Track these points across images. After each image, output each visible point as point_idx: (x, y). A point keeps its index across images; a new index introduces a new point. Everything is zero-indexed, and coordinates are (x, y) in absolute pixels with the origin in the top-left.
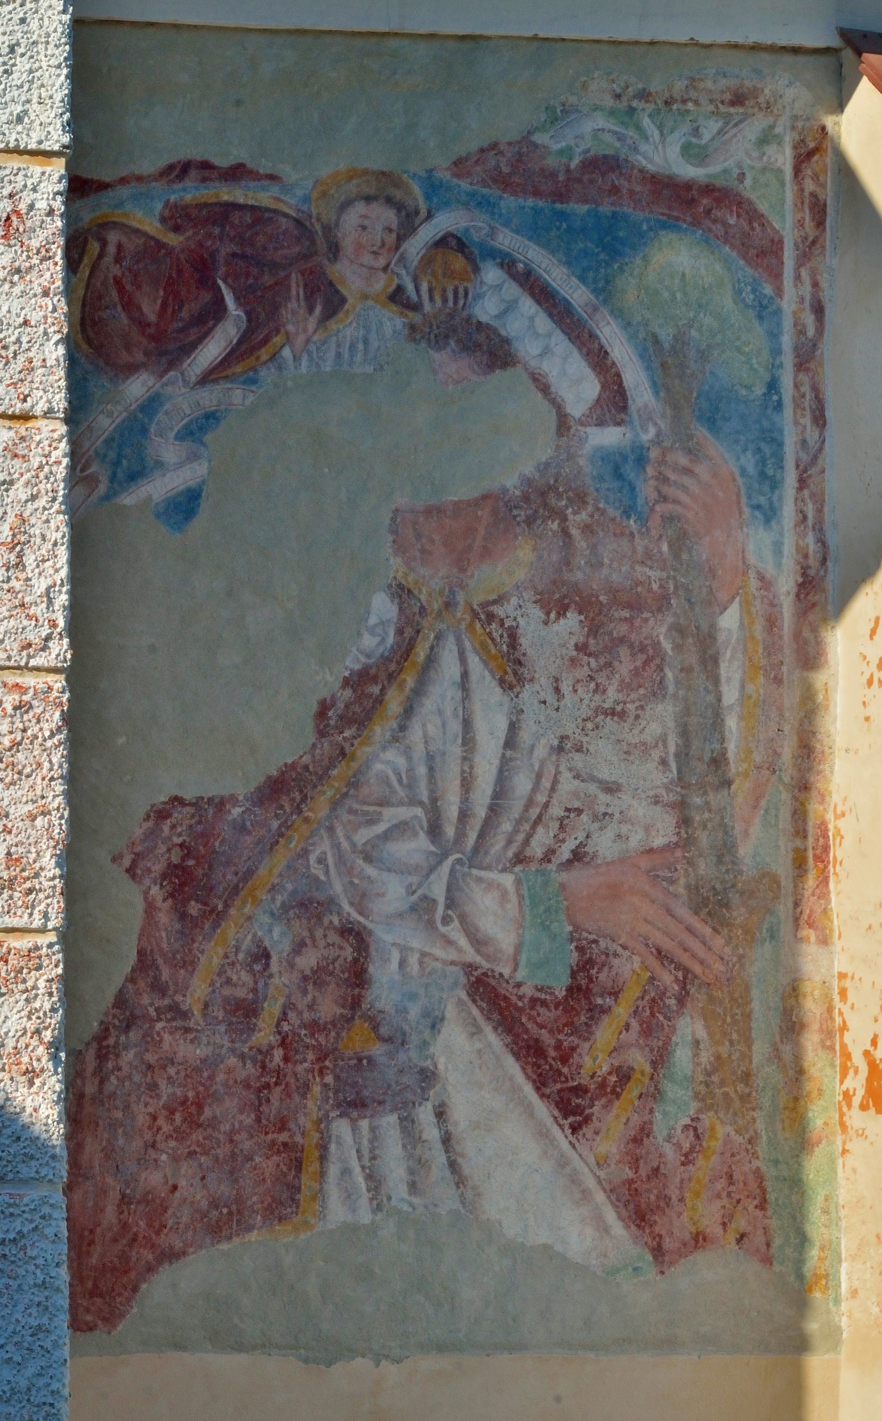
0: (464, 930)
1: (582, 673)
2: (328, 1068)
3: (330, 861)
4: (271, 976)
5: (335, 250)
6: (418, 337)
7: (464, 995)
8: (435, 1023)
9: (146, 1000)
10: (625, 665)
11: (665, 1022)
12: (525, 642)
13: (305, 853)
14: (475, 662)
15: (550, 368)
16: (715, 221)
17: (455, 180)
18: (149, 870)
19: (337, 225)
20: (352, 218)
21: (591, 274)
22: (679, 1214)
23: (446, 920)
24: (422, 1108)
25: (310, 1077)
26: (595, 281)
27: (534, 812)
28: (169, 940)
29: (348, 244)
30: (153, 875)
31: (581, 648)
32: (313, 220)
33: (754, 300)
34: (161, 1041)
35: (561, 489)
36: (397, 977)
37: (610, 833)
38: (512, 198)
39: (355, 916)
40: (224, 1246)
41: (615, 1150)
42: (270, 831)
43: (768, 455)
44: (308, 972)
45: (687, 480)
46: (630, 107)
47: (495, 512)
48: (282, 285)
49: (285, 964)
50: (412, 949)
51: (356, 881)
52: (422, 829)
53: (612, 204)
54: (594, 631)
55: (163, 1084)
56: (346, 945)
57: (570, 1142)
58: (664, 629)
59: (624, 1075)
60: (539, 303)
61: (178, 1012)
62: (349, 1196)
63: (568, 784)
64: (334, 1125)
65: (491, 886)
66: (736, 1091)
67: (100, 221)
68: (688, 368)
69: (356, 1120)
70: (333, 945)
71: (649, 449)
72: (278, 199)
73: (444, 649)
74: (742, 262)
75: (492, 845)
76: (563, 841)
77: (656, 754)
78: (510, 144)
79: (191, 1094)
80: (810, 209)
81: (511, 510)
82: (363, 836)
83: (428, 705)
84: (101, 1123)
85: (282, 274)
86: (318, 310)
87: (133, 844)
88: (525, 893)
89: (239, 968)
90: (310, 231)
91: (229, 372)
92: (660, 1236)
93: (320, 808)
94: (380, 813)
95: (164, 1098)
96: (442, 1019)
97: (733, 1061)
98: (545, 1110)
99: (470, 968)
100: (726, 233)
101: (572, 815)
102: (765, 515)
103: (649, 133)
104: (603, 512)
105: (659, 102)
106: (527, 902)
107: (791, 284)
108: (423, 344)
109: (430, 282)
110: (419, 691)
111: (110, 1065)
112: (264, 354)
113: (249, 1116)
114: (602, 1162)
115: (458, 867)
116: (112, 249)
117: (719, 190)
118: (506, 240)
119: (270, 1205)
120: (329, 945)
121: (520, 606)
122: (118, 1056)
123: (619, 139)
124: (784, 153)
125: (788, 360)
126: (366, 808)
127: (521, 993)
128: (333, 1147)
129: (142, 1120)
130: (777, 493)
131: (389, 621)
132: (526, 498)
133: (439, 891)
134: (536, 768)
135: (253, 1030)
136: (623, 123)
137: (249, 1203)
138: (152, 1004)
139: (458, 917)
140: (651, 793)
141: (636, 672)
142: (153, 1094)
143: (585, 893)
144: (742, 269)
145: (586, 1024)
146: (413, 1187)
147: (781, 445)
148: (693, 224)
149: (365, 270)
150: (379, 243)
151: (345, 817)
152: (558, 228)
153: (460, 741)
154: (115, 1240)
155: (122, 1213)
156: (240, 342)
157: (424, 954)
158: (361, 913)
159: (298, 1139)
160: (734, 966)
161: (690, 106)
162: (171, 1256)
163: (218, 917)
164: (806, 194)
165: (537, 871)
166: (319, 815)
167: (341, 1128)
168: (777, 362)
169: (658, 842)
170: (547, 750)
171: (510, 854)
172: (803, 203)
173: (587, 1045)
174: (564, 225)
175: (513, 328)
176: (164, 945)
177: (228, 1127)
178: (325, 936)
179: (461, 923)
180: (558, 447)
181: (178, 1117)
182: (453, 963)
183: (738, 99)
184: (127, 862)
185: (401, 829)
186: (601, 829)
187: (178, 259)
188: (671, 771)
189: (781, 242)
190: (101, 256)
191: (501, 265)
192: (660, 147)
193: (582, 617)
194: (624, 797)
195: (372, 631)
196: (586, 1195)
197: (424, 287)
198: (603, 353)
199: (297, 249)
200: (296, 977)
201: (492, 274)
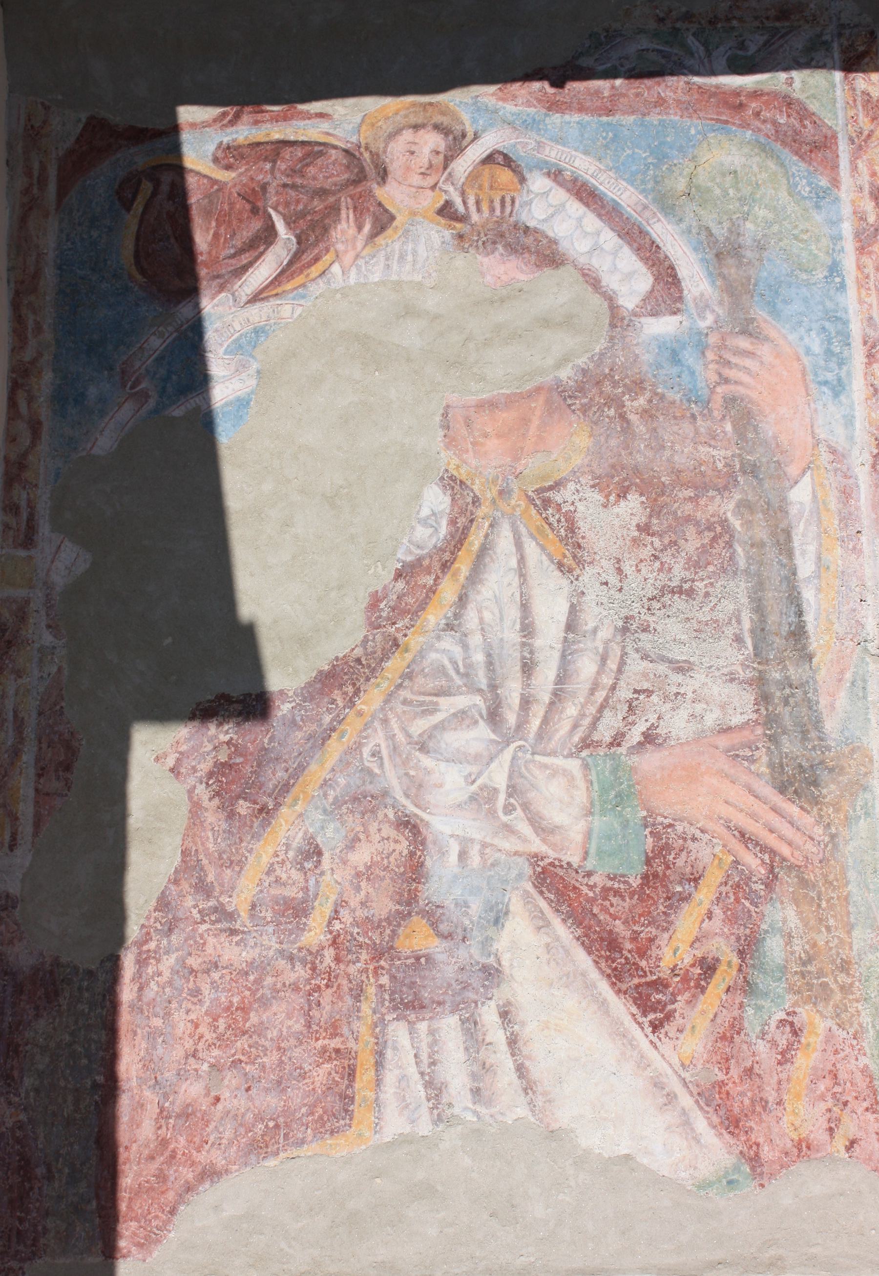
0: (528, 819)
1: (646, 553)
2: (383, 968)
3: (385, 753)
4: (322, 873)
5: (383, 175)
6: (466, 246)
7: (529, 887)
9: (189, 902)
10: (692, 543)
11: (752, 908)
12: (583, 526)
13: (359, 746)
14: (531, 548)
15: (601, 265)
16: (764, 121)
17: (500, 103)
18: (194, 770)
19: (385, 152)
21: (640, 177)
22: (779, 1119)
23: (509, 809)
24: (485, 1008)
25: (364, 978)
26: (643, 182)
27: (600, 696)
28: (216, 840)
29: (395, 167)
30: (198, 774)
31: (645, 528)
32: (362, 150)
33: (810, 192)
34: (204, 944)
35: (617, 377)
36: (456, 870)
37: (683, 714)
38: (558, 115)
39: (411, 808)
40: (272, 1162)
41: (701, 1049)
42: (321, 725)
43: (833, 334)
44: (361, 868)
45: (748, 362)
46: (674, 28)
47: (548, 402)
49: (337, 860)
50: (472, 840)
51: (412, 773)
52: (482, 717)
53: (659, 114)
54: (655, 509)
55: (206, 989)
56: (401, 838)
57: (651, 1042)
58: (731, 506)
59: (709, 967)
60: (587, 205)
61: (224, 914)
63: (636, 665)
64: (391, 1028)
65: (555, 772)
66: (836, 981)
67: (153, 164)
68: (744, 257)
69: (414, 1023)
70: (388, 839)
71: (707, 334)
72: (328, 134)
73: (498, 536)
74: (795, 158)
75: (557, 730)
76: (634, 723)
77: (730, 631)
78: (554, 68)
79: (236, 1000)
80: (863, 106)
81: (565, 399)
84: (139, 1031)
85: (331, 199)
86: (367, 228)
87: (178, 743)
88: (594, 777)
89: (289, 866)
90: (359, 159)
91: (279, 290)
92: (758, 1145)
94: (436, 704)
95: (208, 1004)
96: (507, 913)
97: (831, 949)
98: (622, 1007)
99: (535, 858)
100: (777, 131)
101: (642, 697)
102: (833, 389)
103: (694, 49)
104: (662, 397)
105: (703, 22)
106: (596, 786)
107: (848, 175)
108: (472, 251)
109: (477, 195)
111: (150, 970)
112: (314, 271)
113: (297, 1022)
114: (687, 1063)
115: (520, 754)
116: (165, 188)
117: (768, 94)
118: (553, 153)
119: (321, 1118)
120: (383, 839)
121: (578, 491)
122: (158, 961)
123: (664, 57)
124: (833, 57)
125: (849, 245)
126: (422, 698)
127: (591, 883)
128: (389, 1054)
129: (182, 1027)
130: (845, 368)
131: (443, 511)
132: (581, 388)
133: (500, 780)
134: (601, 650)
135: (304, 930)
136: (666, 43)
137: (298, 1115)
138: (195, 906)
139: (521, 805)
140: (725, 671)
141: (704, 550)
142: (195, 1000)
143: (658, 776)
144: (796, 165)
145: (664, 913)
146: (476, 1092)
147: (846, 323)
148: (741, 126)
149: (414, 190)
150: (426, 165)
151: (400, 708)
152: (605, 138)
153: (518, 627)
154: (152, 1158)
155: (160, 1128)
156: (291, 263)
157: (484, 845)
158: (416, 806)
159: (351, 1044)
160: (826, 846)
161: (735, 23)
163: (265, 813)
164: (858, 93)
165: (606, 755)
166: (373, 708)
168: (838, 248)
169: (737, 720)
170: (611, 630)
171: (576, 739)
172: (855, 101)
173: (666, 935)
174: (610, 134)
176: (211, 846)
177: (275, 1033)
178: (379, 830)
179: (524, 810)
180: (612, 338)
181: (222, 1024)
182: (516, 853)
183: (784, 14)
184: (171, 762)
185: (461, 717)
186: (673, 709)
187: (231, 193)
188: (746, 648)
189: (834, 137)
190: (154, 194)
191: (548, 174)
192: (706, 60)
193: (644, 499)
194: (697, 676)
195: (424, 522)
196: (671, 1098)
197: (471, 201)
198: (655, 247)
199: (346, 176)
200: (349, 873)
201: (538, 183)
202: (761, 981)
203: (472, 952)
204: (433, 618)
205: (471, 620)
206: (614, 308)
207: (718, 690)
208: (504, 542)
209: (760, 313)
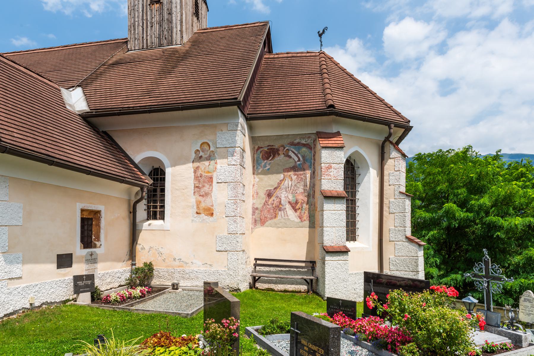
5: (279, 151)
8: (286, 205)
15: (294, 158)
20: (280, 148)
29: (280, 150)
59: (299, 208)
62: (280, 217)
63: (296, 188)
83: (285, 183)
93: (278, 190)
110: (285, 181)
118: (291, 149)
162: (267, 221)
163: (271, 198)
167: (279, 212)
175: (292, 155)
201: (290, 151)
202: (303, 209)
203: (284, 207)
204: (282, 184)
205: (285, 184)
206: (295, 161)
207: (301, 190)
208: (287, 179)
209: (306, 162)
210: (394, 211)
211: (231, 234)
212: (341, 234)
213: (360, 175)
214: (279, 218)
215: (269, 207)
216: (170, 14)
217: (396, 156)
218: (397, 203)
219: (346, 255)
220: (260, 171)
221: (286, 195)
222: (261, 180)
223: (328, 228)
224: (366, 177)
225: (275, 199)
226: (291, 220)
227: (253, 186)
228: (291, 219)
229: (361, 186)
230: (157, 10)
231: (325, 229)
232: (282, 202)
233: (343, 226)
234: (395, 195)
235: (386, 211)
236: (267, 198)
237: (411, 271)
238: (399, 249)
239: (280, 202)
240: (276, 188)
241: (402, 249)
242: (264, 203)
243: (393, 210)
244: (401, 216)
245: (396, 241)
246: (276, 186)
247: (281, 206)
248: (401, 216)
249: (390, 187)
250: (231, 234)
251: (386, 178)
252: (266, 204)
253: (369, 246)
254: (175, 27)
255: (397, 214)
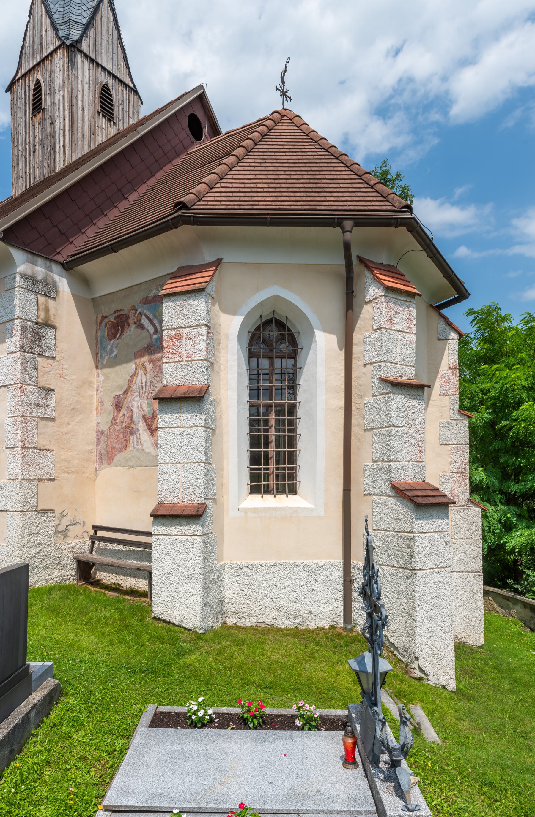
48: (124, 324)
82: (133, 397)
162: (116, 455)
163: (120, 410)
203: (137, 427)
204: (134, 383)
205: (137, 383)
208: (140, 372)
210: (373, 425)
211: (11, 479)
212: (195, 478)
213: (302, 349)
214: (131, 449)
215: (117, 428)
216: (52, 123)
217: (376, 296)
218: (376, 405)
219: (195, 524)
220: (105, 362)
221: (139, 404)
222: (107, 377)
223: (166, 465)
224: (311, 351)
225: (126, 412)
226: (146, 453)
227: (97, 390)
228: (146, 450)
229: (303, 373)
230: (39, 124)
231: (161, 468)
232: (135, 418)
233: (199, 461)
234: (373, 386)
235: (359, 425)
236: (116, 411)
237: (402, 568)
238: (379, 513)
239: (132, 417)
240: (126, 392)
241: (385, 514)
242: (112, 422)
243: (370, 422)
244: (383, 435)
245: (375, 495)
246: (125, 387)
247: (133, 426)
248: (383, 435)
249: (364, 370)
250: (11, 479)
251: (355, 350)
252: (114, 422)
253: (315, 505)
254: (57, 142)
255: (376, 431)
